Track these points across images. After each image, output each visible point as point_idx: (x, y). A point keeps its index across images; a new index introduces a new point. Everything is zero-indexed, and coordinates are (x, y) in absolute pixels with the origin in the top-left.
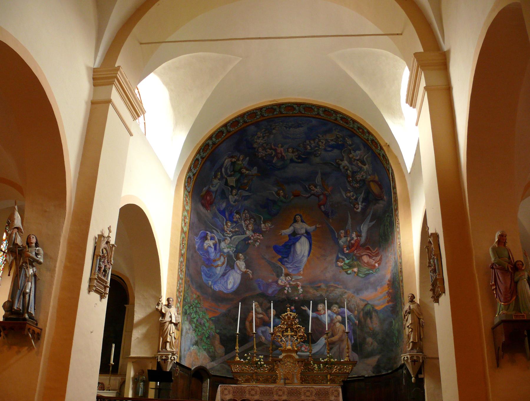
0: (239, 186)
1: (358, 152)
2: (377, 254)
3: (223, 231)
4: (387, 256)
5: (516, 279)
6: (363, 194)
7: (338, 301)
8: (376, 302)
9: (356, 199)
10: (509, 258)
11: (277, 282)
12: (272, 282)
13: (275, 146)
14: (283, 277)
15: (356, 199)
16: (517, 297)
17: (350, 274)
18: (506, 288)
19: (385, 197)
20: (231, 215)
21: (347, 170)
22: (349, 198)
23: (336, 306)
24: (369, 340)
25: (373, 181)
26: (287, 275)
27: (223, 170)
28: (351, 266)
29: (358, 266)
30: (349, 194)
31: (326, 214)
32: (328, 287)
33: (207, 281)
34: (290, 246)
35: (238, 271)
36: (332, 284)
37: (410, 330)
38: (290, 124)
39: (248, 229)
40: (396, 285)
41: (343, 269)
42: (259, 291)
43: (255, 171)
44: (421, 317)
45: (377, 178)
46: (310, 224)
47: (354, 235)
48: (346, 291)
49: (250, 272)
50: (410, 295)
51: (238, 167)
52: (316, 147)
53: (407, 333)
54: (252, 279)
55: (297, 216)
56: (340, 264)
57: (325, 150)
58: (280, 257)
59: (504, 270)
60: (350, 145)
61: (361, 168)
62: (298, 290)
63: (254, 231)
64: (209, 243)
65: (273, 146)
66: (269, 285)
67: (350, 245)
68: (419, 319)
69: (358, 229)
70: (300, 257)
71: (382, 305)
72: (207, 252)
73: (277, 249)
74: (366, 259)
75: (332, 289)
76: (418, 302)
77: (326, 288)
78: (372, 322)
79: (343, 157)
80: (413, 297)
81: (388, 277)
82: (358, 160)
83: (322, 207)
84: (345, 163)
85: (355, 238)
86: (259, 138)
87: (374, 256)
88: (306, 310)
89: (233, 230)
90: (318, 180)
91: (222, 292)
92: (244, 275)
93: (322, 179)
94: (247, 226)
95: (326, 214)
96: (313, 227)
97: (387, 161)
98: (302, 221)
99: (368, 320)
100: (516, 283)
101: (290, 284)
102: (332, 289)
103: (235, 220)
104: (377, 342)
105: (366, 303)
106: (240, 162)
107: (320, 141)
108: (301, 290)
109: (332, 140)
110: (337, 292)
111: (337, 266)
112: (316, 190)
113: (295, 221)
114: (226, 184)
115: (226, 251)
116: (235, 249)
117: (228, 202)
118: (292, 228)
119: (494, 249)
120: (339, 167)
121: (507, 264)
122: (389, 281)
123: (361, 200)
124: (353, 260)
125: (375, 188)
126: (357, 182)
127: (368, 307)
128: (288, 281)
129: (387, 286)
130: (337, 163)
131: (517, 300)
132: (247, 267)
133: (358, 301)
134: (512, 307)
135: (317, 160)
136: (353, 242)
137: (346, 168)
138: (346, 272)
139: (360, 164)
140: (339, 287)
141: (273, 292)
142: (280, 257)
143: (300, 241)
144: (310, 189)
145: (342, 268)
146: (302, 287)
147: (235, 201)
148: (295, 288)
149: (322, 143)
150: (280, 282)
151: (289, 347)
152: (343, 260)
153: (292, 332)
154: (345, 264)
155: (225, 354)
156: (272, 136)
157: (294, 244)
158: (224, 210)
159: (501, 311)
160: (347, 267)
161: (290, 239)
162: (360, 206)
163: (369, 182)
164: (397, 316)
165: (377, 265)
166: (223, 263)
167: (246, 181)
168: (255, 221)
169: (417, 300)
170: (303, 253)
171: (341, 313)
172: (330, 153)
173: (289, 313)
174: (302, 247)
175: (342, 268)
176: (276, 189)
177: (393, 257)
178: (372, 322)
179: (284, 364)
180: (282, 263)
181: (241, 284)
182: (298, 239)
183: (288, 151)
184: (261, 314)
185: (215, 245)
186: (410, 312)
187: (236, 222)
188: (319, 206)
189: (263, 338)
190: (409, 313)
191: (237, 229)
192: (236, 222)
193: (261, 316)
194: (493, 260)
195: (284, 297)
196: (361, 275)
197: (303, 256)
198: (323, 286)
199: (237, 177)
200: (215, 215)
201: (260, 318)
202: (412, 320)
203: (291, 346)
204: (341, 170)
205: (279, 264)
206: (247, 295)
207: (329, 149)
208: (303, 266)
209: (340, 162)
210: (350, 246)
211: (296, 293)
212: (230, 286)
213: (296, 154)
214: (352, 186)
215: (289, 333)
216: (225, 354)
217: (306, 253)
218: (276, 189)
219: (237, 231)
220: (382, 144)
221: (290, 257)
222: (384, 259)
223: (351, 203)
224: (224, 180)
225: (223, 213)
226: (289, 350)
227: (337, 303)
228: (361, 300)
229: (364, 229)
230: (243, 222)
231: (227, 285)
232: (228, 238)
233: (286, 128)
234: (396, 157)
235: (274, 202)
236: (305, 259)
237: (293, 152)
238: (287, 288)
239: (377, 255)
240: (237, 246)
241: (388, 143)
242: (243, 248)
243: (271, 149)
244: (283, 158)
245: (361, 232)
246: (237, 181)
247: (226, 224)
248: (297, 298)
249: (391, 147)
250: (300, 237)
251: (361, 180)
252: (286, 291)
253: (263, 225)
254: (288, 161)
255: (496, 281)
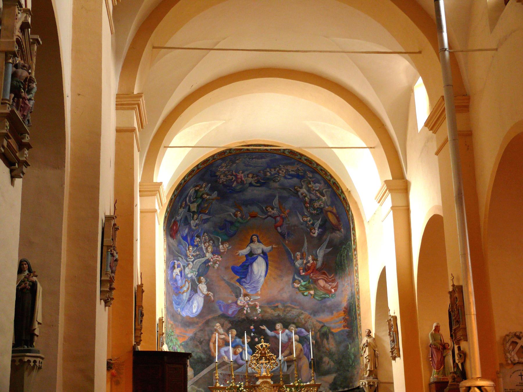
0: (200, 210)
1: (317, 184)
2: (333, 280)
3: (186, 256)
4: (343, 285)
5: (444, 355)
6: (320, 220)
7: (295, 321)
8: (332, 325)
9: (313, 224)
10: (441, 340)
11: (236, 303)
12: (232, 303)
13: (236, 172)
14: (241, 298)
15: (313, 224)
16: (444, 366)
17: (306, 296)
18: (438, 361)
19: (342, 230)
20: (192, 239)
21: (305, 197)
22: (306, 222)
23: (294, 325)
24: (326, 359)
25: (331, 212)
26: (245, 295)
27: (188, 199)
28: (307, 289)
29: (315, 289)
30: (306, 219)
31: (282, 235)
32: (286, 307)
33: (177, 308)
34: (248, 266)
35: (201, 295)
36: (289, 305)
37: (368, 360)
38: (254, 157)
39: (207, 251)
40: (351, 313)
41: (300, 291)
42: (220, 312)
43: (215, 195)
44: (376, 349)
45: (335, 211)
46: (267, 245)
47: (310, 258)
48: (303, 311)
49: (211, 294)
50: (367, 331)
51: (200, 194)
52: (276, 174)
53: (365, 363)
54: (213, 301)
55: (254, 237)
56: (296, 285)
57: (285, 177)
58: (238, 277)
59: (437, 349)
60: (311, 178)
61: (319, 198)
62: (257, 310)
63: (213, 253)
64: (177, 271)
65: (234, 173)
66: (228, 306)
67: (307, 268)
68: (375, 351)
69: (314, 253)
70: (258, 277)
71: (338, 328)
72: (176, 281)
73: (235, 270)
74: (322, 283)
75: (289, 309)
76: (374, 336)
77: (283, 308)
78: (328, 344)
79: (302, 185)
80: (370, 332)
81: (345, 304)
82: (316, 191)
83: (279, 228)
84: (304, 190)
85: (311, 262)
86: (222, 167)
87: (330, 282)
88: (264, 330)
89: (195, 254)
90: (276, 202)
91: (189, 316)
92: (206, 297)
93: (279, 202)
94: (207, 249)
95: (282, 235)
96: (270, 247)
97: (347, 203)
98: (259, 241)
99: (325, 341)
100: (444, 357)
101: (248, 305)
102: (289, 309)
103: (196, 243)
104: (333, 361)
105: (322, 325)
106: (203, 189)
107: (280, 169)
108: (259, 310)
109: (292, 171)
110: (294, 313)
111: (294, 287)
112: (273, 212)
113: (252, 241)
114: (189, 210)
115: (189, 276)
116: (197, 273)
117: (190, 228)
118: (248, 248)
119: (432, 334)
120: (297, 193)
121: (439, 345)
122: (345, 308)
123: (318, 226)
124: (309, 282)
125: (332, 218)
126: (314, 209)
127: (325, 329)
128: (246, 301)
129: (343, 313)
130: (295, 190)
131: (444, 368)
132: (208, 290)
133: (315, 323)
134: (441, 373)
135: (276, 185)
136: (309, 264)
137: (304, 195)
138: (303, 294)
139: (318, 194)
140: (296, 307)
141: (233, 312)
142: (238, 277)
143: (256, 261)
144: (267, 210)
145: (299, 289)
146: (261, 307)
147: (197, 225)
148: (253, 308)
149: (283, 171)
150: (239, 302)
151: (264, 374)
152: (300, 281)
153: (266, 360)
154: (301, 285)
155: (195, 376)
156: (235, 165)
157: (251, 264)
158: (187, 235)
159: (434, 376)
160: (304, 289)
161: (247, 260)
162: (317, 231)
163: (327, 211)
164: (353, 342)
165: (333, 290)
166: (188, 289)
167: (206, 205)
168: (214, 243)
169: (373, 334)
170: (260, 273)
171: (299, 333)
172: (290, 181)
173: (263, 343)
174: (259, 267)
175: (299, 289)
176: (234, 211)
177: (349, 289)
178: (328, 344)
179: (262, 389)
180: (240, 283)
181: (204, 307)
182: (255, 259)
183: (248, 177)
184: (223, 334)
185: (181, 272)
186: (368, 345)
187: (197, 246)
188: (276, 228)
189: (226, 358)
190: (367, 346)
191: (198, 253)
192: (197, 246)
193: (223, 336)
194: (431, 342)
195: (243, 317)
196: (317, 298)
197: (260, 276)
198: (280, 306)
199: (199, 203)
200: (180, 243)
201: (222, 339)
202: (369, 352)
203: (266, 372)
204: (299, 196)
205: (238, 284)
206: (210, 317)
207: (289, 177)
208: (260, 285)
209: (299, 189)
210: (306, 269)
211: (255, 313)
212: (194, 311)
213: (256, 178)
214: (309, 212)
215: (263, 361)
216: (195, 376)
217: (263, 273)
218: (234, 211)
219: (198, 255)
220: (344, 190)
221: (248, 278)
222: (340, 286)
223: (307, 227)
224: (188, 207)
225: (185, 238)
226: (265, 377)
227: (294, 323)
228: (317, 321)
229: (321, 253)
230: (203, 244)
231: (192, 310)
232: (191, 263)
233: (249, 159)
234: (356, 203)
235: (232, 223)
236: (262, 280)
237: (252, 178)
238: (246, 309)
239: (333, 281)
240: (199, 269)
241: (349, 189)
242: (204, 270)
243: (232, 175)
244: (242, 182)
245: (317, 256)
246: (198, 206)
247: (189, 249)
248: (256, 318)
249: (352, 193)
250: (257, 258)
251: (318, 208)
252: (245, 312)
253: (221, 246)
254: (248, 185)
255: (432, 357)
